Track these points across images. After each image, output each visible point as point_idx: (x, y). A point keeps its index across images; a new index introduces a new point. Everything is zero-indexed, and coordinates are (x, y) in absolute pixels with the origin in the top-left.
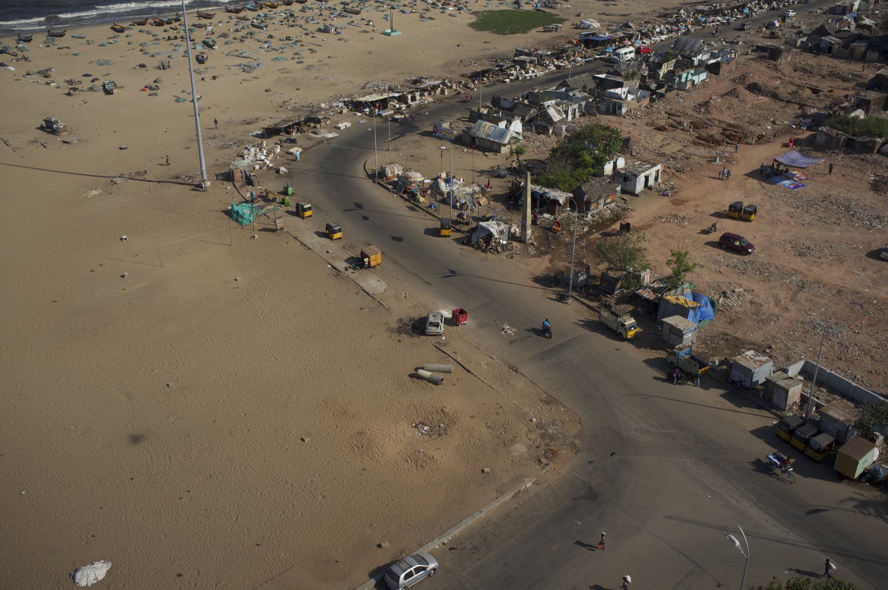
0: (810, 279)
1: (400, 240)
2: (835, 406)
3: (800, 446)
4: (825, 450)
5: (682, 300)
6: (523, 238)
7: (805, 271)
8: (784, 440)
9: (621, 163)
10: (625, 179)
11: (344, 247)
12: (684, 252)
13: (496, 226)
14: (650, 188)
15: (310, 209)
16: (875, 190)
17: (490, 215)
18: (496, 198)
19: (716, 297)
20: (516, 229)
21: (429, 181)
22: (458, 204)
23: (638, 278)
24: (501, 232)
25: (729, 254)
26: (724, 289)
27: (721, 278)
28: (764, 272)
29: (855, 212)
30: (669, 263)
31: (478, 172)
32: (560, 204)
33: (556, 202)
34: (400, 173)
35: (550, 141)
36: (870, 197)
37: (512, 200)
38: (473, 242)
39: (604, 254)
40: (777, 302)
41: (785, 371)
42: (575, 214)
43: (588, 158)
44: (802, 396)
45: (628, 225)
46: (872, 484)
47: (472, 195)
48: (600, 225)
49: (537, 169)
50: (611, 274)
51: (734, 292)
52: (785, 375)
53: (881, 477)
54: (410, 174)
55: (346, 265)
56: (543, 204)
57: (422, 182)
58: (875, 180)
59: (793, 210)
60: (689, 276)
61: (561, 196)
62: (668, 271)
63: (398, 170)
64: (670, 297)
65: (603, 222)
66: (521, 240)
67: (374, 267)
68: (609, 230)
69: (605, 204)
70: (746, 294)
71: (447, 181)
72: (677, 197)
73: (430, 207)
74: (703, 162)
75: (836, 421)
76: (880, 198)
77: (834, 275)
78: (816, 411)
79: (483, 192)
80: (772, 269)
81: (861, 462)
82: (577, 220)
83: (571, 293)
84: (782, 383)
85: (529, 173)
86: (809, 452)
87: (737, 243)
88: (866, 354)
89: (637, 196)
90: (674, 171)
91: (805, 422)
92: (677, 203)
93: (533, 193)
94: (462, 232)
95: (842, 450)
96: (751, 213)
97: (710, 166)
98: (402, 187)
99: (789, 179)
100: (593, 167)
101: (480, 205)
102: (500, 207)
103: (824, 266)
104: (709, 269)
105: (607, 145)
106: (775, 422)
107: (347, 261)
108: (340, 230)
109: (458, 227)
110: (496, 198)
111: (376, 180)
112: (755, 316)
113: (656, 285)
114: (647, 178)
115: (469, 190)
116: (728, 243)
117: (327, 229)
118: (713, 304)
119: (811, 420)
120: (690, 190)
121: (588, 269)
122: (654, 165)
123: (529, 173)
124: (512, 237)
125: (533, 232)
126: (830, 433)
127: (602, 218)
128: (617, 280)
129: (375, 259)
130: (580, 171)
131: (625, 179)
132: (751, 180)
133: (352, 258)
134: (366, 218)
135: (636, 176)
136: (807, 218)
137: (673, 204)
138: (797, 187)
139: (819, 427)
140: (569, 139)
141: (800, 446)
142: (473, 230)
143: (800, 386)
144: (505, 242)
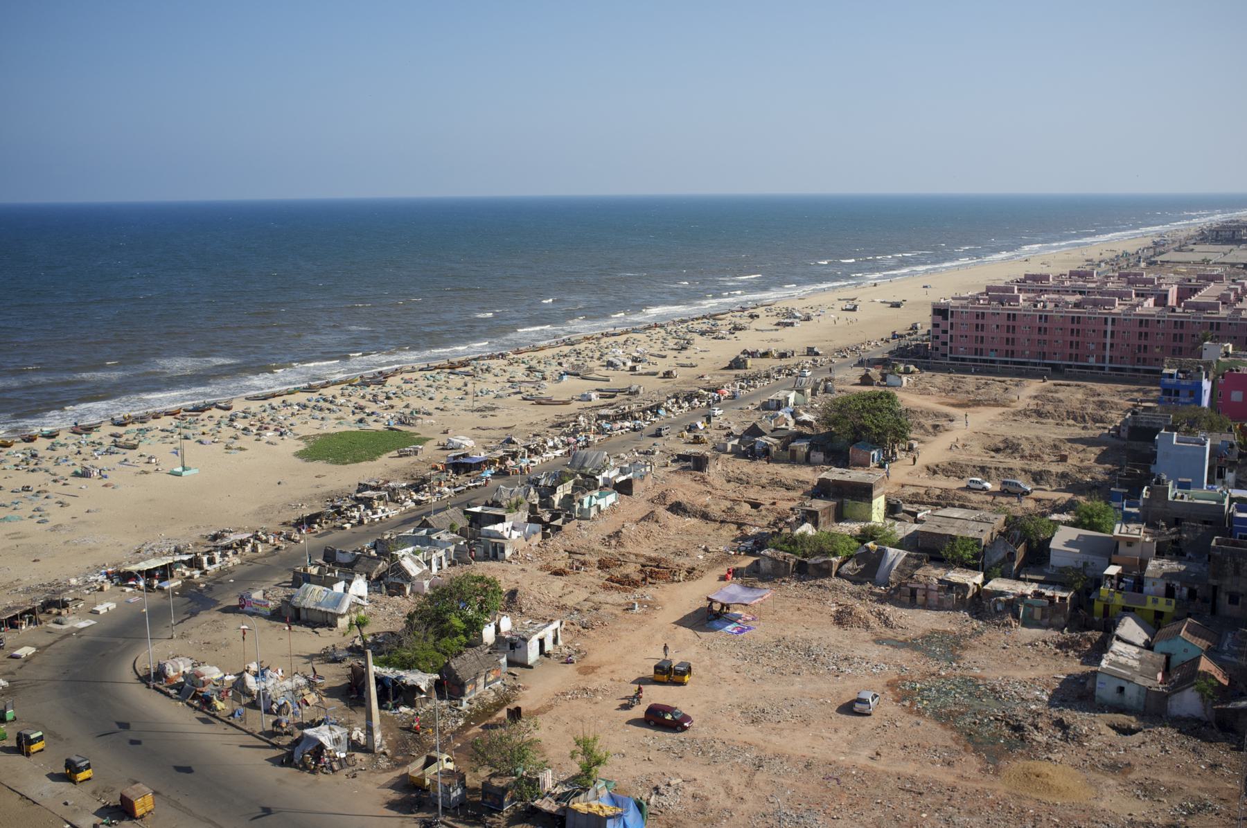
0: (769, 753)
1: (188, 770)
5: (595, 809)
6: (370, 747)
7: (761, 743)
9: (506, 624)
10: (512, 646)
11: (94, 793)
12: (591, 737)
13: (327, 733)
14: (548, 655)
15: (40, 739)
17: (320, 718)
18: (331, 692)
19: (646, 796)
20: (359, 734)
21: (232, 677)
22: (275, 707)
23: (533, 783)
24: (337, 741)
25: (659, 733)
26: (656, 782)
27: (650, 769)
28: (707, 752)
29: (818, 655)
30: (572, 757)
31: (306, 657)
32: (421, 692)
33: (415, 689)
34: (187, 670)
35: (407, 603)
36: (834, 634)
37: (353, 693)
38: (296, 761)
39: (483, 755)
40: (728, 791)
42: (445, 703)
43: (457, 623)
45: (518, 709)
47: (294, 692)
48: (482, 714)
49: (385, 647)
50: (495, 782)
51: (669, 785)
54: (202, 669)
55: (97, 820)
56: (394, 693)
57: (221, 680)
59: (739, 663)
60: (601, 772)
61: (422, 680)
62: (575, 769)
63: (185, 666)
64: (579, 805)
65: (484, 711)
66: (367, 749)
67: (142, 817)
68: (493, 720)
69: (486, 684)
70: (685, 785)
71: (256, 675)
72: (585, 663)
73: (233, 715)
74: (618, 612)
76: (846, 633)
77: (798, 743)
79: (311, 685)
80: (718, 746)
82: (448, 710)
83: (441, 818)
85: (369, 651)
87: (669, 717)
89: (531, 667)
90: (579, 627)
92: (587, 671)
93: (380, 681)
94: (281, 747)
96: (683, 674)
97: (627, 616)
98: (192, 692)
99: (731, 622)
100: (466, 633)
101: (307, 704)
102: (335, 704)
103: (786, 733)
104: (631, 757)
105: (483, 602)
107: (99, 813)
108: (88, 767)
109: (274, 741)
110: (331, 692)
111: (152, 684)
112: (700, 816)
113: (559, 790)
114: (541, 642)
115: (288, 684)
116: (658, 719)
117: (67, 766)
118: (639, 806)
120: (600, 650)
121: (463, 778)
122: (551, 621)
123: (369, 651)
124: (354, 746)
125: (384, 736)
127: (482, 704)
128: (504, 790)
129: (142, 805)
130: (446, 641)
131: (512, 646)
132: (682, 629)
133: (107, 807)
134: (138, 742)
135: (525, 640)
136: (758, 670)
137: (580, 673)
138: (742, 631)
140: (431, 599)
142: (296, 743)
144: (343, 755)
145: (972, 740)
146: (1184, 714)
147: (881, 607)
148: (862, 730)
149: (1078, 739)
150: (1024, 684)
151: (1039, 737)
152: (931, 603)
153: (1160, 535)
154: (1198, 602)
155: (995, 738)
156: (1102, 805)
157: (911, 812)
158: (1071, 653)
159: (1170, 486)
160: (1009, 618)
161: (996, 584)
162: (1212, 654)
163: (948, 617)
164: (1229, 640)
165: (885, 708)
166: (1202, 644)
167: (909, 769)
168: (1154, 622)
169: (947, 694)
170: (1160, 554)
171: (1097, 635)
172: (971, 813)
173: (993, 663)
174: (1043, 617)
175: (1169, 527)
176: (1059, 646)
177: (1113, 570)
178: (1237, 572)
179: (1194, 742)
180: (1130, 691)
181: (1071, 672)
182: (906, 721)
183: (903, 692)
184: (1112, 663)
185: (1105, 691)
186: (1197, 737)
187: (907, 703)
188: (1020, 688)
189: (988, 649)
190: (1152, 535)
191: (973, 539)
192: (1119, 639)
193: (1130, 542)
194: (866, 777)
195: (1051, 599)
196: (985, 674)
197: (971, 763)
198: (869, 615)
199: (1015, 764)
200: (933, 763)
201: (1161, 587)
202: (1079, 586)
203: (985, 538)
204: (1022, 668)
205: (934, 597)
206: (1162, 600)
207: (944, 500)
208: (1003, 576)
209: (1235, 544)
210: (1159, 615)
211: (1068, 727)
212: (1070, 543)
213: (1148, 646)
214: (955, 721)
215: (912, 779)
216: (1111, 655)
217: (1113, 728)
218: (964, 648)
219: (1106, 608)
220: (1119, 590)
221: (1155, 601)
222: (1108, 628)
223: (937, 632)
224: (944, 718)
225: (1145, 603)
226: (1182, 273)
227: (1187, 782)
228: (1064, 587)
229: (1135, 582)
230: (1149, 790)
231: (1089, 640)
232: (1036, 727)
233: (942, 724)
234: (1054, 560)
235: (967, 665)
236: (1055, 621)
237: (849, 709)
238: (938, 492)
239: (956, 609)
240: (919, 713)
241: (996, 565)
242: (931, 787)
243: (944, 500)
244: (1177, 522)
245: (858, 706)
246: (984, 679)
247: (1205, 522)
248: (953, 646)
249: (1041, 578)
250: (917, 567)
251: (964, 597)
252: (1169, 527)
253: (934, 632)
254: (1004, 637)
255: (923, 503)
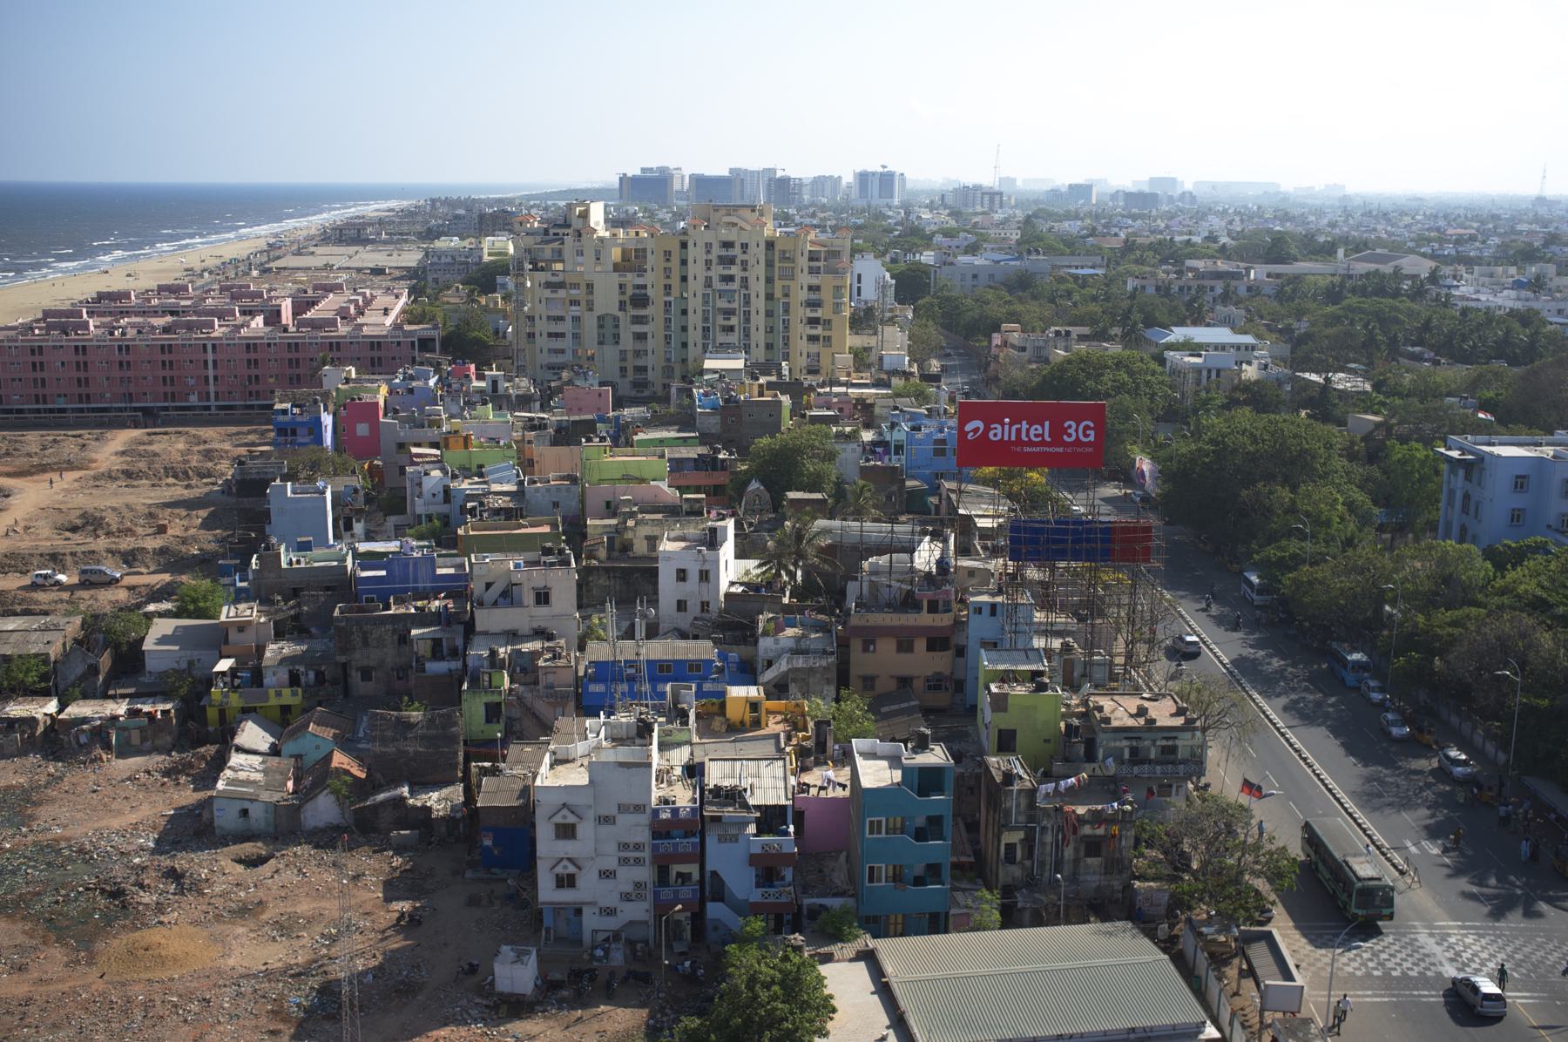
226: (301, 282)
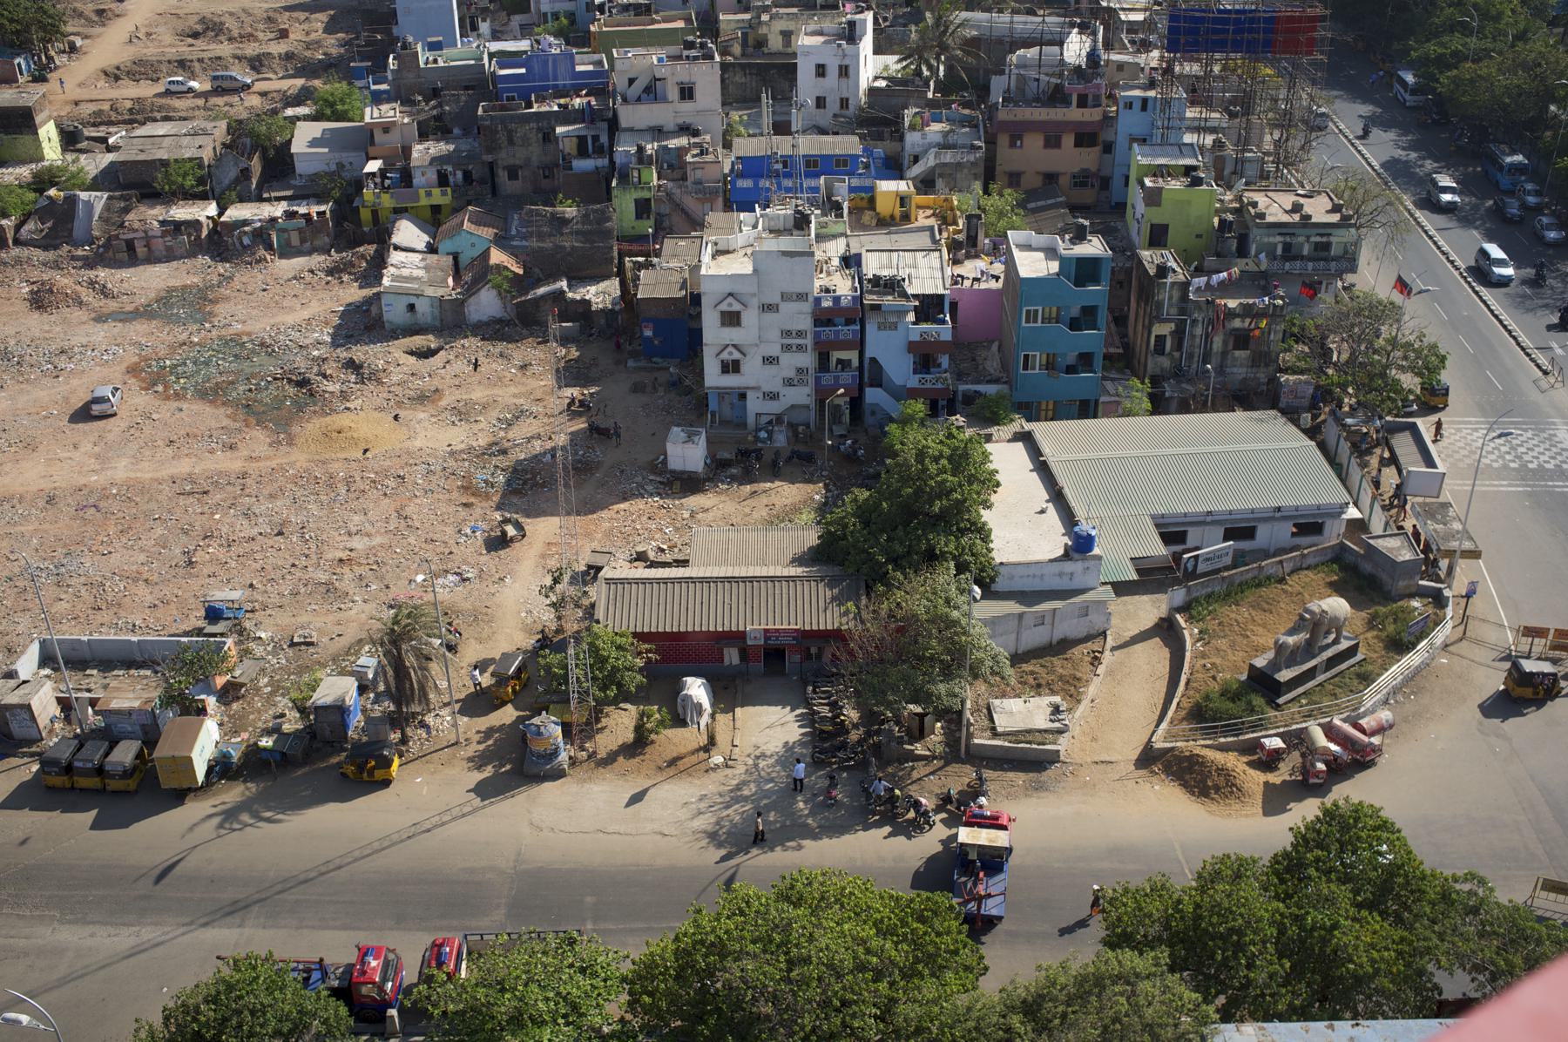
2: (118, 689)
3: (93, 782)
4: (135, 769)
8: (62, 790)
16: (39, 308)
36: (36, 323)
41: (11, 675)
44: (59, 700)
46: (229, 779)
52: (12, 683)
53: (235, 760)
58: (32, 292)
75: (129, 713)
76: (53, 318)
78: (96, 713)
81: (195, 755)
84: (13, 699)
86: (113, 785)
88: (136, 580)
91: (81, 741)
95: (162, 751)
106: (35, 767)
119: (92, 731)
126: (129, 736)
139: (109, 736)
141: (93, 782)
143: (49, 685)
145: (252, 412)
146: (485, 318)
147: (92, 274)
148: (110, 437)
149: (375, 377)
150: (298, 328)
151: (332, 387)
152: (157, 254)
153: (419, 112)
154: (478, 185)
155: (278, 402)
156: (418, 443)
157: (199, 517)
158: (346, 278)
159: (419, 49)
160: (262, 252)
161: (235, 213)
162: (501, 241)
163: (184, 267)
164: (515, 223)
165: (133, 401)
166: (488, 233)
167: (183, 467)
168: (433, 220)
169: (207, 363)
170: (423, 136)
171: (369, 249)
172: (272, 496)
173: (254, 312)
174: (303, 241)
175: (427, 101)
176: (330, 272)
177: (373, 166)
178: (511, 142)
179: (500, 347)
180: (423, 307)
181: (350, 300)
182: (164, 411)
183: (152, 375)
184: (395, 278)
185: (394, 313)
186: (502, 340)
187: (160, 388)
188: (295, 335)
189: (243, 295)
190: (410, 114)
191: (191, 159)
192: (397, 248)
193: (386, 128)
194: (131, 492)
195: (307, 217)
196: (248, 328)
197: (258, 440)
198: (78, 288)
199: (310, 426)
200: (212, 452)
201: (432, 176)
202: (336, 193)
203: (207, 155)
204: (292, 309)
205: (159, 245)
206: (436, 191)
207: (138, 115)
208: (241, 201)
209: (503, 108)
210: (436, 209)
211: (361, 366)
212: (314, 143)
213: (432, 249)
214: (225, 394)
215: (191, 479)
216: (392, 270)
217: (412, 353)
218: (214, 302)
219: (375, 213)
220: (385, 189)
221: (429, 194)
222: (382, 237)
223: (175, 289)
224: (211, 394)
225: (418, 199)
227: (500, 392)
228: (320, 198)
229: (401, 175)
230: (462, 413)
231: (363, 257)
232: (325, 376)
233: (210, 402)
234: (301, 167)
235: (224, 322)
236: (317, 243)
237: (84, 414)
238: (128, 104)
239: (191, 255)
240: (178, 396)
241: (229, 188)
242: (217, 481)
243: (138, 115)
244: (436, 93)
245: (96, 409)
246: (249, 334)
247: (467, 88)
248: (199, 302)
249: (289, 193)
250: (127, 210)
251: (199, 237)
252: (427, 101)
253: (170, 290)
254: (260, 277)
255: (110, 123)
